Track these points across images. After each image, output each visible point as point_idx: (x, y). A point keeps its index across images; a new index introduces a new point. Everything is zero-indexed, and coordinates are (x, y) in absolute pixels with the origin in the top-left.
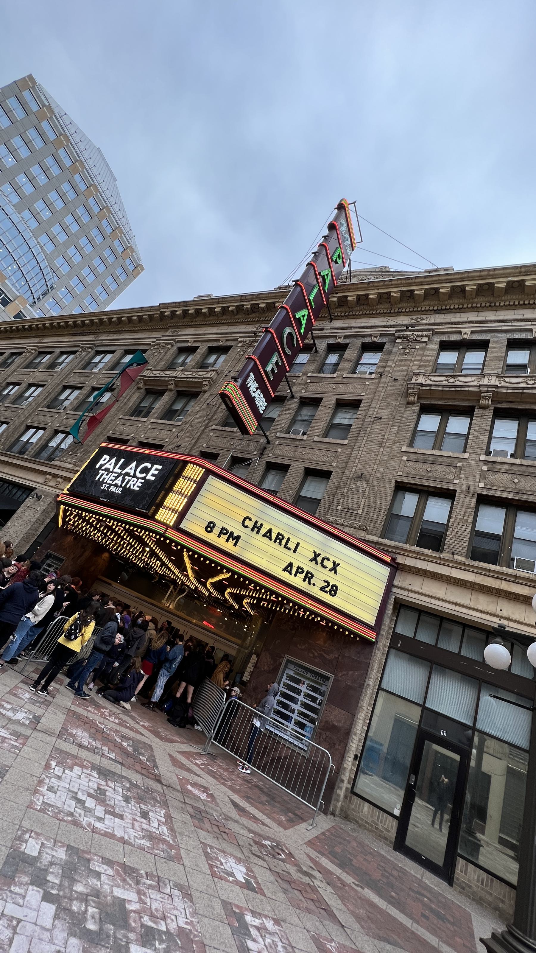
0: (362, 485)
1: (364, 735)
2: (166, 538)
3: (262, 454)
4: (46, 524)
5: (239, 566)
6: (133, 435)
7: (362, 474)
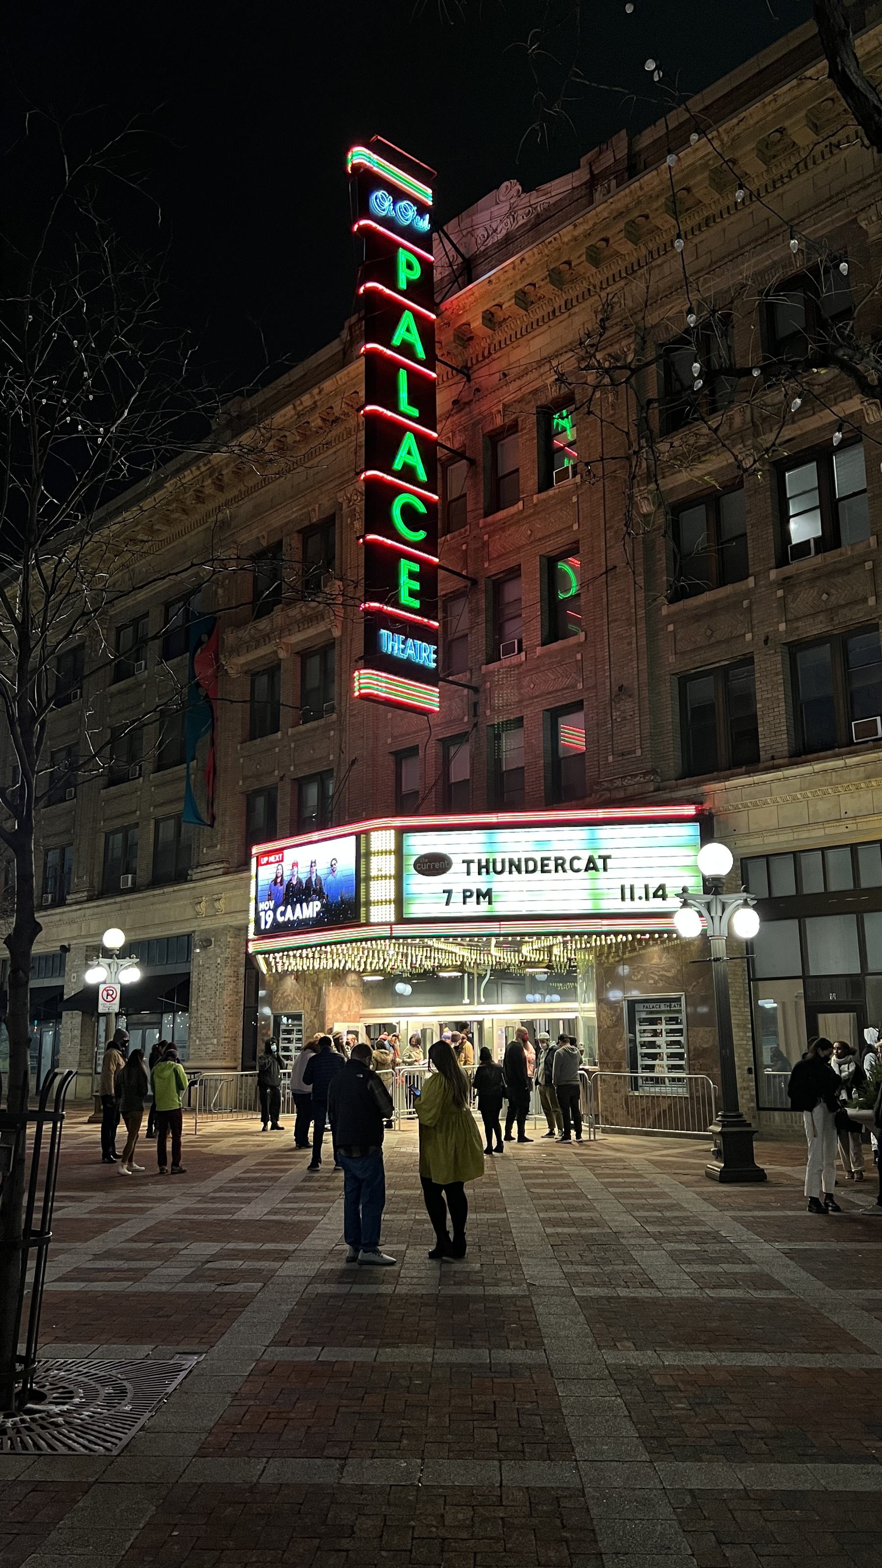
0: (628, 706)
1: (751, 1043)
2: (397, 938)
3: (475, 715)
4: (242, 976)
5: (496, 924)
6: (276, 772)
7: (621, 688)
